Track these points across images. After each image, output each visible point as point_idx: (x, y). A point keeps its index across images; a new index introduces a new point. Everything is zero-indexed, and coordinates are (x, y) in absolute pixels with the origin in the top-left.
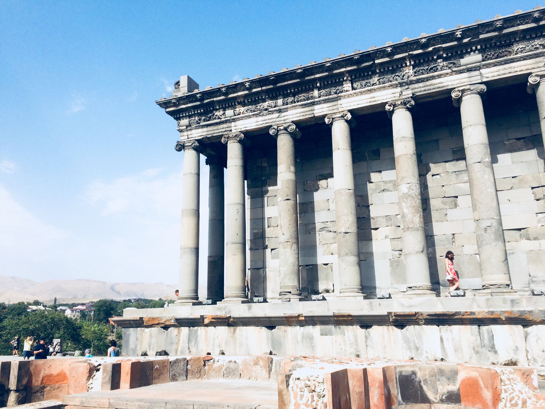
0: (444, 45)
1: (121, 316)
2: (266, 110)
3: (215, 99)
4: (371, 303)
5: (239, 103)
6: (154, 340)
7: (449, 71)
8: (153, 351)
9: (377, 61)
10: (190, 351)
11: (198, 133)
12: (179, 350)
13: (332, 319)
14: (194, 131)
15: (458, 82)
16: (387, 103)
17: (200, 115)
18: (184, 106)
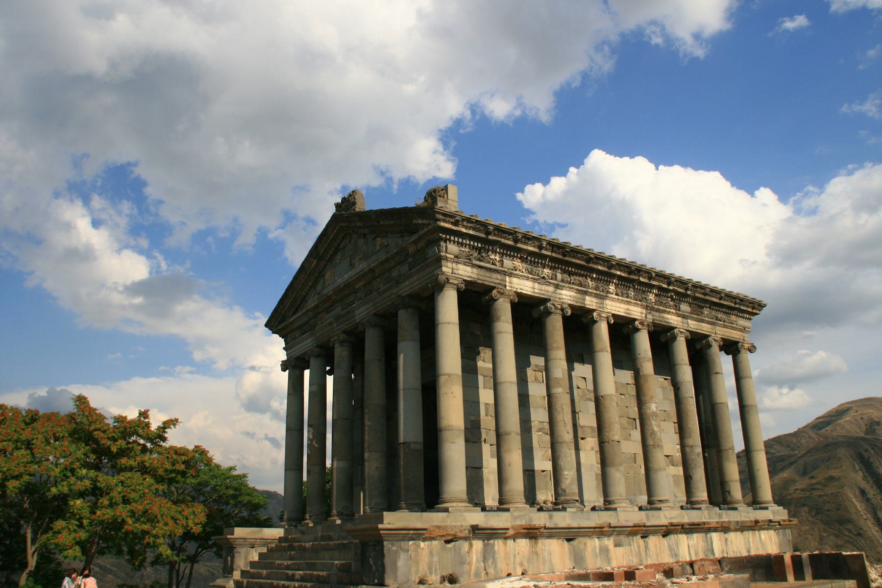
1: (382, 523)
2: (544, 278)
3: (503, 241)
4: (647, 515)
5: (520, 258)
6: (436, 559)
7: (673, 311)
8: (436, 575)
9: (642, 279)
10: (487, 573)
11: (466, 272)
12: (473, 571)
14: (461, 266)
16: (635, 320)
17: (474, 247)
18: (464, 230)
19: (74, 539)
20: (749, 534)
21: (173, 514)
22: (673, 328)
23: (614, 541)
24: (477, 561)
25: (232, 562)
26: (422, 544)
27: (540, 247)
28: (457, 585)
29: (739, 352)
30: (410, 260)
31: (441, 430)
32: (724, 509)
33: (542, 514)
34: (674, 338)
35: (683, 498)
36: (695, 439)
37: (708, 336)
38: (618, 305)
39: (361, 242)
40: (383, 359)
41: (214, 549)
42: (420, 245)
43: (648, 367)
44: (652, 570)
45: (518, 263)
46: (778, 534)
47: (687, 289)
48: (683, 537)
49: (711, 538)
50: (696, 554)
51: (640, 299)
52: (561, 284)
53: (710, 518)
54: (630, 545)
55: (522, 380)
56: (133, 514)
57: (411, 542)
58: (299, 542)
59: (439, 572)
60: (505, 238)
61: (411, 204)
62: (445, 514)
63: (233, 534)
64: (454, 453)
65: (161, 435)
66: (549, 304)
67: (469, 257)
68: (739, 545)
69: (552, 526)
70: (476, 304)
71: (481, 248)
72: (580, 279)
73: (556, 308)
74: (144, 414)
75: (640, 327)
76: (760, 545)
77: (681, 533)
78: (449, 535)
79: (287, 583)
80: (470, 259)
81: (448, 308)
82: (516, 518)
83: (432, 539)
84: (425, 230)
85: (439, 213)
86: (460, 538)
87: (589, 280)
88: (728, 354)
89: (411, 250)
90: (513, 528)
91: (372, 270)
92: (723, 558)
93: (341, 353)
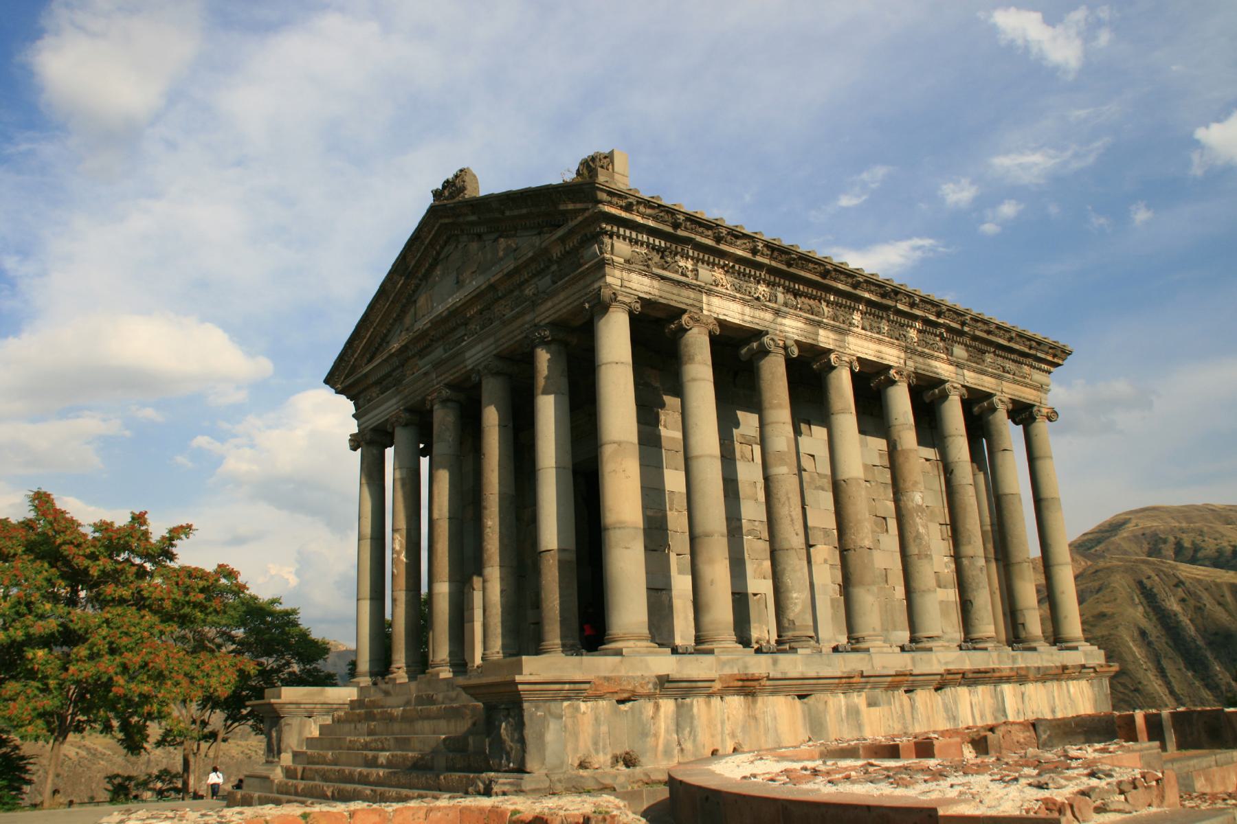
0: (953, 325)
1: (521, 673)
2: (758, 299)
3: (698, 238)
4: (913, 659)
7: (944, 356)
8: (605, 754)
9: (900, 306)
10: (682, 750)
11: (642, 285)
12: (661, 747)
13: (889, 679)
14: (634, 276)
15: (947, 374)
16: (890, 367)
18: (639, 220)
19: (35, 709)
20: (1053, 686)
21: (187, 669)
22: (943, 382)
23: (867, 698)
24: (667, 731)
25: (279, 740)
26: (583, 706)
27: (754, 251)
28: (638, 769)
29: (1032, 419)
30: (554, 268)
31: (606, 529)
32: (1019, 649)
33: (763, 658)
34: (944, 396)
35: (958, 635)
36: (976, 546)
37: (989, 396)
38: (866, 344)
39: (474, 246)
40: (511, 425)
41: (250, 722)
42: (570, 245)
43: (908, 437)
44: (958, 739)
45: (719, 274)
46: (1091, 685)
47: (963, 324)
48: (963, 691)
49: (1002, 693)
50: (982, 717)
51: (898, 336)
52: (784, 309)
53: (1000, 662)
54: (889, 703)
55: (728, 457)
56: (125, 668)
57: (566, 704)
58: (382, 707)
59: (609, 749)
60: (701, 234)
61: (556, 180)
62: (618, 658)
63: (279, 697)
64: (627, 564)
65: (165, 552)
66: (766, 339)
67: (646, 262)
68: (1041, 701)
69: (779, 676)
70: (657, 337)
71: (666, 248)
72: (811, 302)
73: (777, 346)
74: (139, 519)
75: (897, 377)
76: (1067, 701)
77: (960, 685)
78: (623, 691)
79: (365, 771)
80: (648, 266)
81: (615, 340)
82: (724, 664)
83: (600, 697)
84: (580, 218)
85: (602, 190)
86: (641, 696)
87: (824, 304)
88: (1017, 423)
89: (556, 252)
90: (721, 679)
91: (492, 287)
92: (1038, 719)
93: (444, 419)
